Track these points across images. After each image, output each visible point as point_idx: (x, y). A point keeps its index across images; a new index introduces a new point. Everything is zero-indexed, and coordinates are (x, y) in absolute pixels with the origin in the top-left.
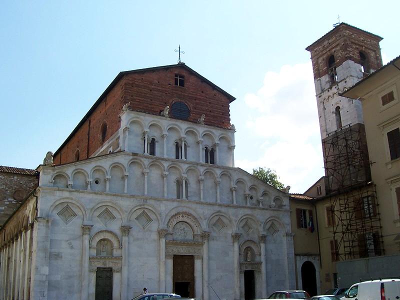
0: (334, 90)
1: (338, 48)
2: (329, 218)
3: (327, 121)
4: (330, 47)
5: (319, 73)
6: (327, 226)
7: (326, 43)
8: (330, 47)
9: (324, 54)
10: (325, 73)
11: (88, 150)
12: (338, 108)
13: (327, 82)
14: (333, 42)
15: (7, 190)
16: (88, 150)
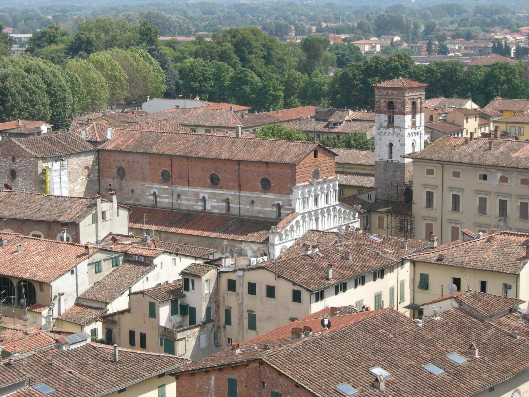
0: (391, 130)
1: (398, 101)
2: (379, 223)
3: (381, 149)
4: (393, 97)
5: (380, 111)
6: (377, 227)
7: (390, 92)
8: (393, 97)
9: (386, 99)
10: (385, 113)
11: (240, 186)
12: (391, 145)
13: (385, 121)
14: (397, 95)
15: (78, 170)
16: (240, 186)
